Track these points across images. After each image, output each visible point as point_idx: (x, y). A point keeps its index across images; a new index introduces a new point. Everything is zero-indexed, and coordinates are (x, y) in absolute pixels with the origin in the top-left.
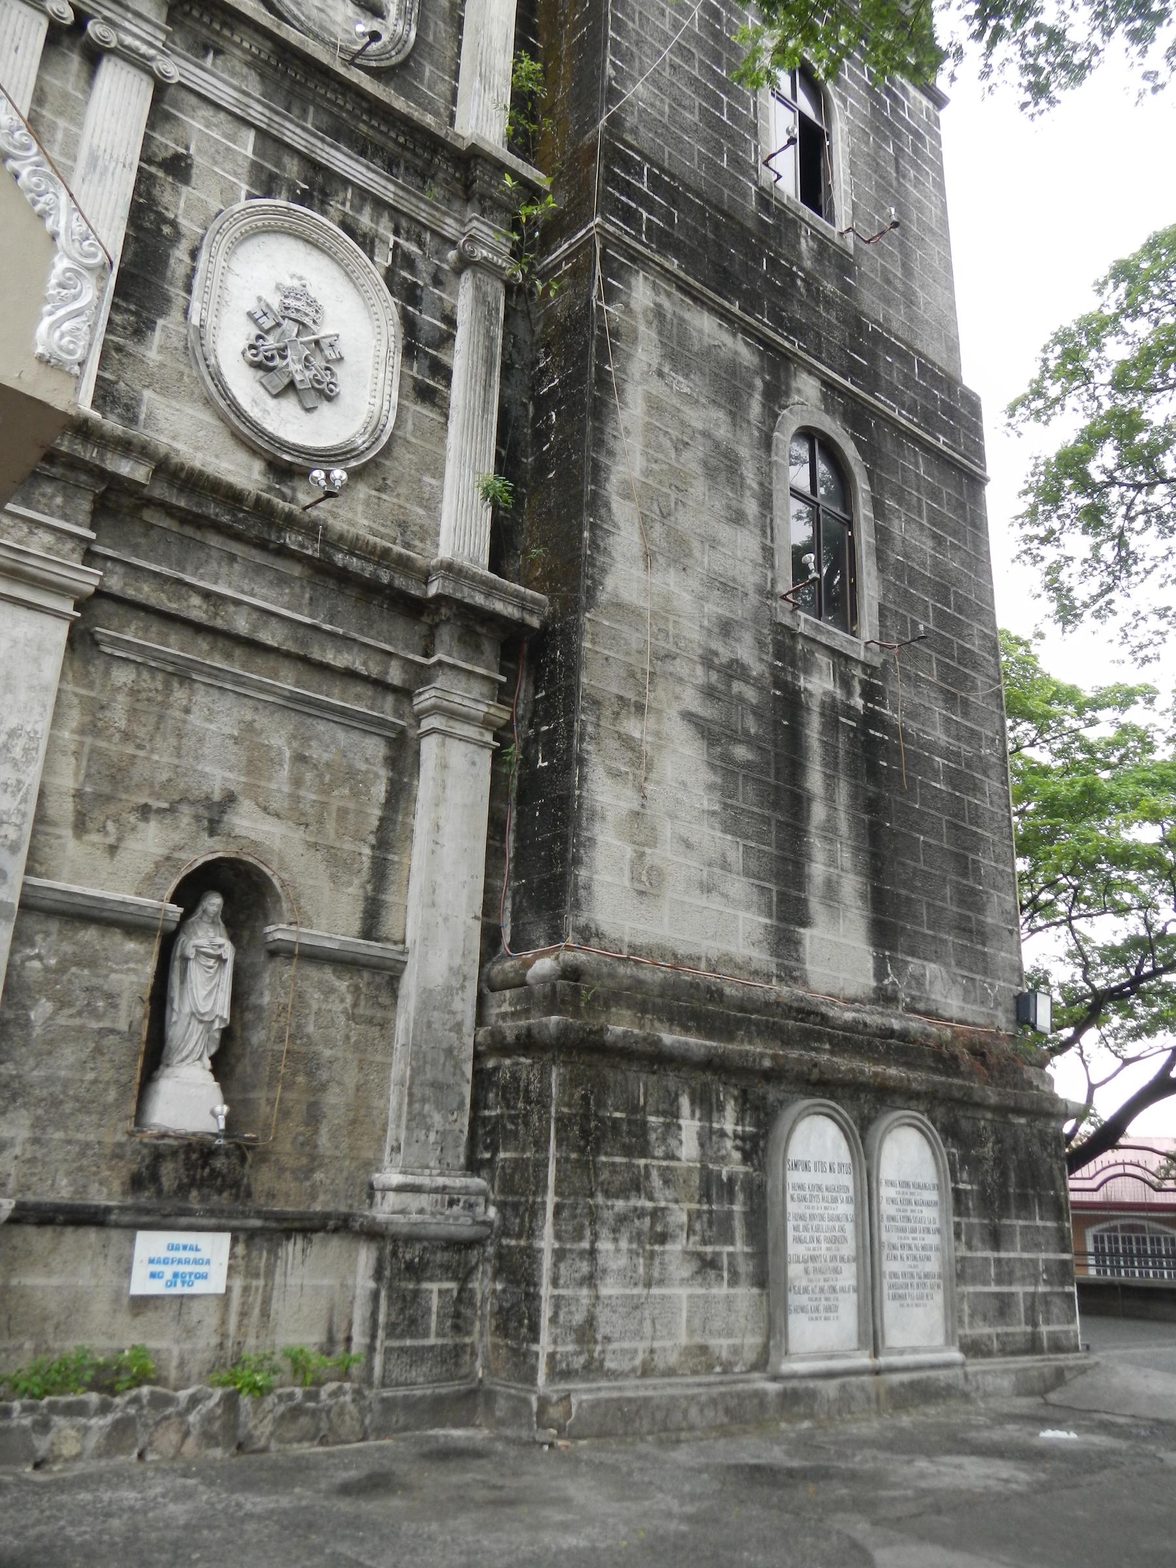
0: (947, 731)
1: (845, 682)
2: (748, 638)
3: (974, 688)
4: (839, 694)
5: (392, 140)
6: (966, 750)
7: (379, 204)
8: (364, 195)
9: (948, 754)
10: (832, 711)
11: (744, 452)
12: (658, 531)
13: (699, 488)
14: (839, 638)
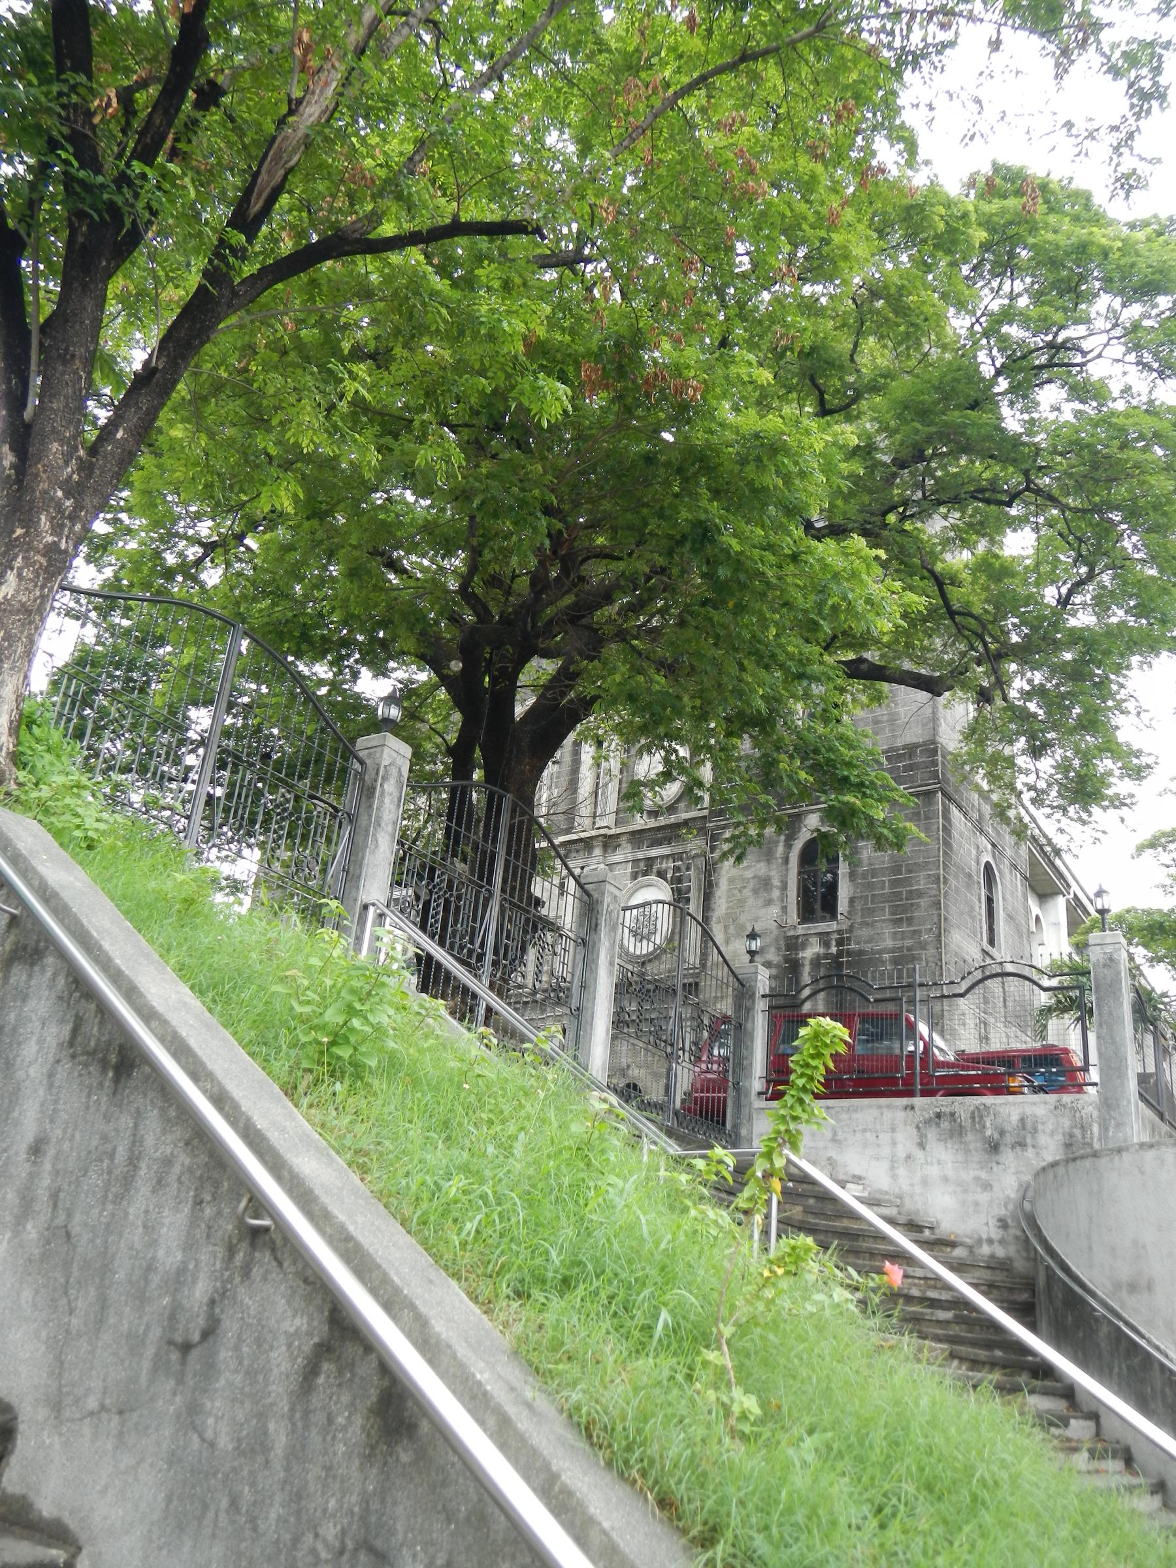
0: (894, 939)
1: (827, 945)
2: (772, 949)
3: (919, 906)
4: (822, 951)
5: (667, 833)
6: (909, 942)
7: (667, 856)
8: (663, 857)
9: (893, 951)
10: (816, 962)
11: (773, 873)
12: (732, 929)
13: (751, 902)
14: (822, 927)
